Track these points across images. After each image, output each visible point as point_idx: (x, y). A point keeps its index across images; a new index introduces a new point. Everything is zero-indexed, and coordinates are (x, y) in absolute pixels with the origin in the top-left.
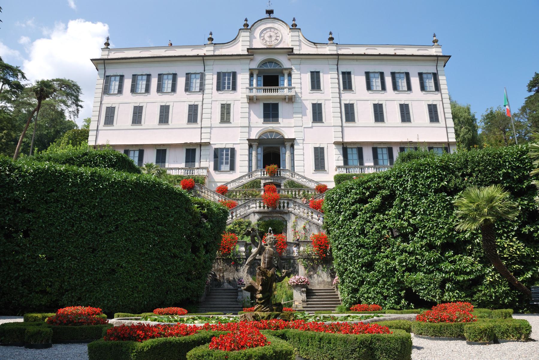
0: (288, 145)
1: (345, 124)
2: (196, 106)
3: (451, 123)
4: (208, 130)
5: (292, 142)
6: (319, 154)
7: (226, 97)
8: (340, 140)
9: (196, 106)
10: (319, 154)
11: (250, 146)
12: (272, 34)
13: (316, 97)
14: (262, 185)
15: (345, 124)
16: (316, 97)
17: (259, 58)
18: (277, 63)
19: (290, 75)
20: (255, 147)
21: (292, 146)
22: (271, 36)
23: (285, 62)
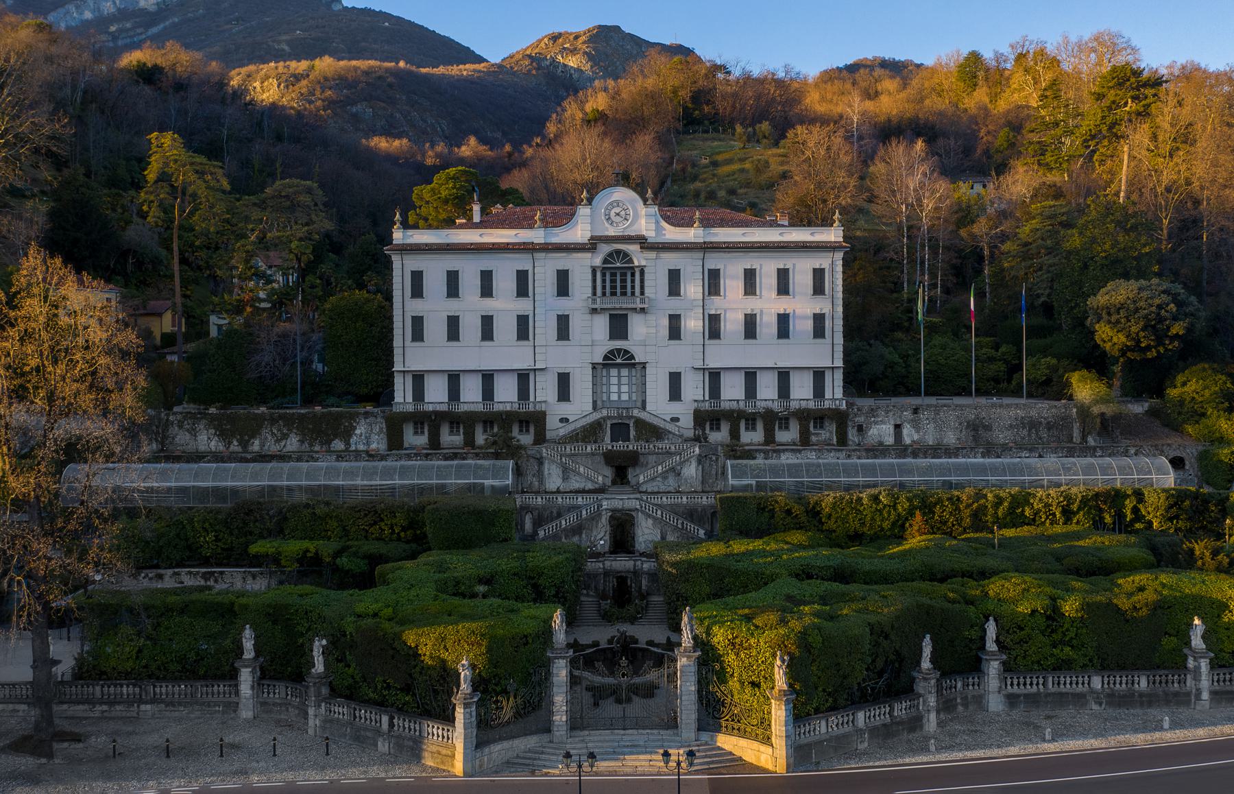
0: (639, 367)
1: (707, 342)
2: (528, 316)
3: (839, 339)
4: (543, 350)
5: (644, 366)
6: (675, 380)
7: (564, 305)
8: (699, 364)
9: (528, 316)
10: (675, 380)
11: (594, 368)
12: (617, 210)
13: (674, 305)
14: (609, 426)
15: (707, 342)
16: (674, 305)
17: (605, 249)
18: (626, 255)
19: (642, 273)
20: (599, 371)
21: (644, 367)
22: (618, 214)
23: (639, 258)
